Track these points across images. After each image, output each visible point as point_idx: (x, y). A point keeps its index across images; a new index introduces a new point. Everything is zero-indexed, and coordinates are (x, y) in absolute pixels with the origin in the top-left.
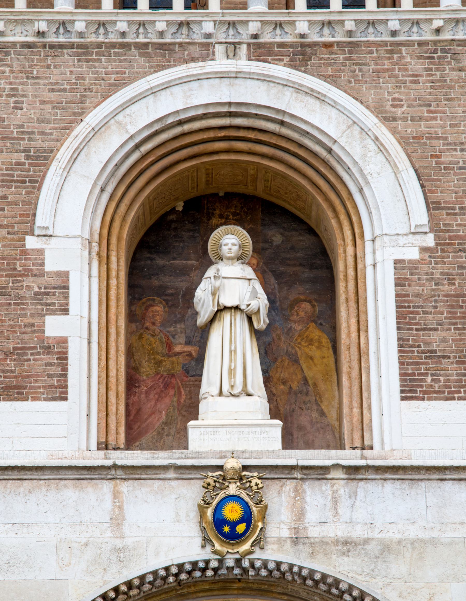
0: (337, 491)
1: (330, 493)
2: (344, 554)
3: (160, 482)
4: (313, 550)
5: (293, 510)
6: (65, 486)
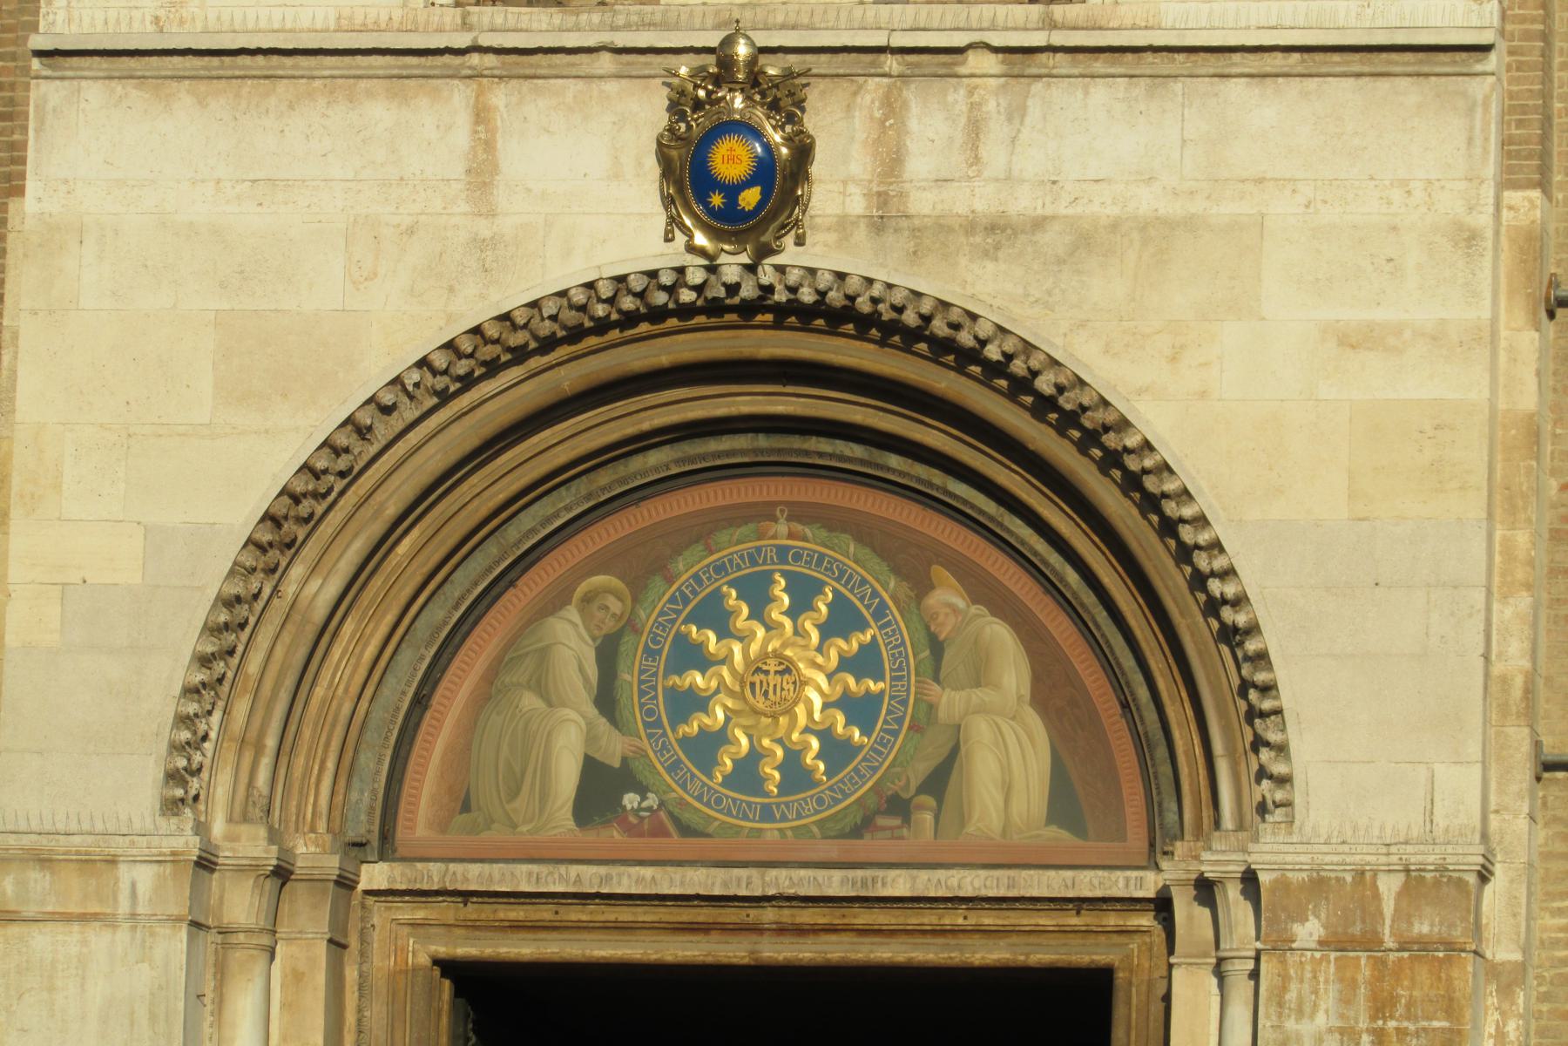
0: (980, 104)
1: (965, 108)
2: (987, 255)
3: (580, 84)
4: (917, 245)
5: (877, 150)
6: (370, 94)
